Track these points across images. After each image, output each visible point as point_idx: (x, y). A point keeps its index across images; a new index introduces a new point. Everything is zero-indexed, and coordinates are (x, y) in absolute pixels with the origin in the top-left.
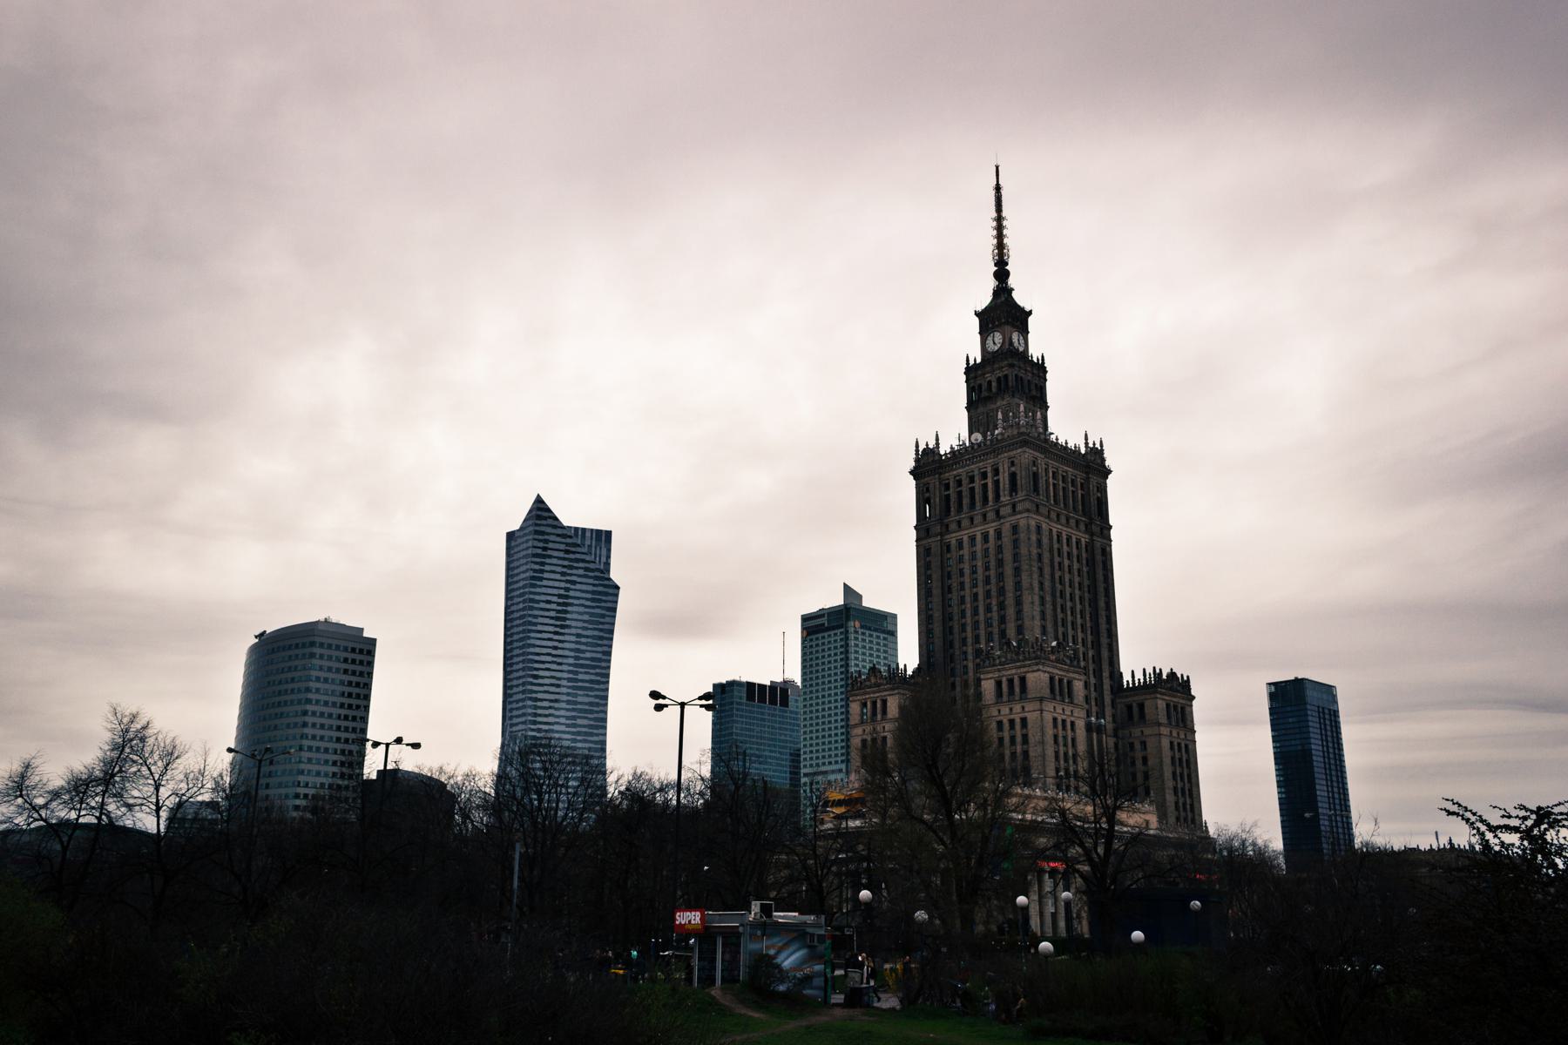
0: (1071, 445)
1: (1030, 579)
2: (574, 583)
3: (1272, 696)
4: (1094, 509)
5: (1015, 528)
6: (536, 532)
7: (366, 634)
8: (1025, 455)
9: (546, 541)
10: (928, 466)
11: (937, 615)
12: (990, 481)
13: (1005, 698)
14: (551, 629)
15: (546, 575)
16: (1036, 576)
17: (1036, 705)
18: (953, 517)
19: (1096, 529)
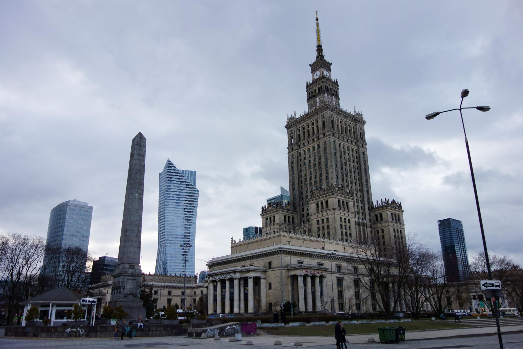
0: (348, 111)
1: (331, 163)
2: (182, 190)
3: (440, 225)
4: (359, 136)
5: (325, 142)
6: (168, 172)
7: (89, 205)
8: (328, 113)
9: (172, 175)
10: (292, 124)
11: (296, 181)
12: (315, 126)
13: (320, 210)
14: (175, 206)
15: (172, 187)
16: (333, 161)
17: (332, 212)
18: (302, 142)
19: (360, 144)
